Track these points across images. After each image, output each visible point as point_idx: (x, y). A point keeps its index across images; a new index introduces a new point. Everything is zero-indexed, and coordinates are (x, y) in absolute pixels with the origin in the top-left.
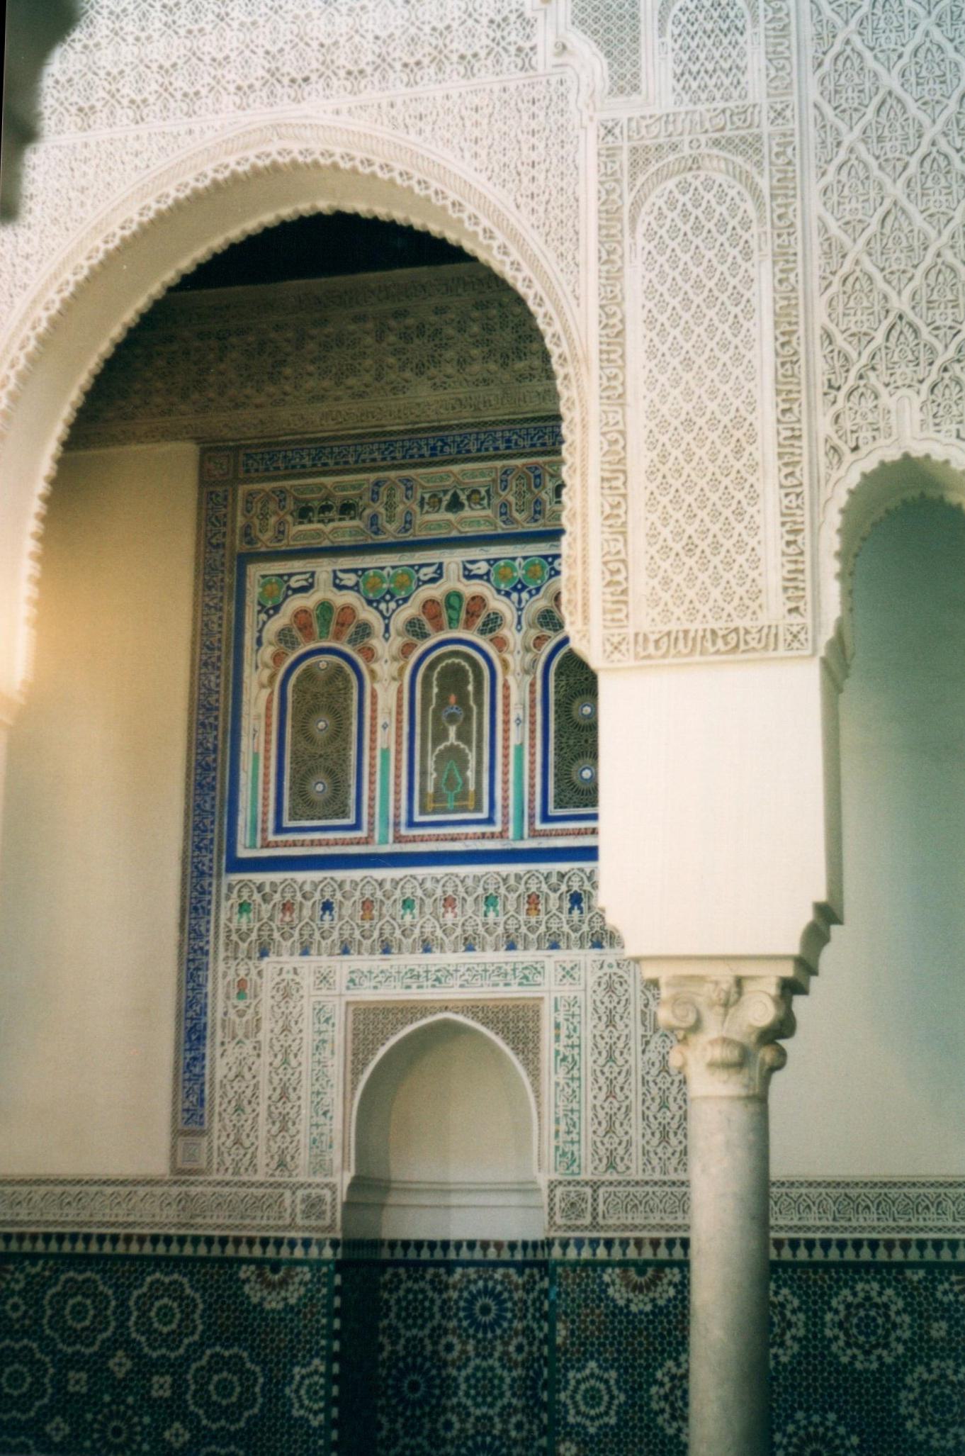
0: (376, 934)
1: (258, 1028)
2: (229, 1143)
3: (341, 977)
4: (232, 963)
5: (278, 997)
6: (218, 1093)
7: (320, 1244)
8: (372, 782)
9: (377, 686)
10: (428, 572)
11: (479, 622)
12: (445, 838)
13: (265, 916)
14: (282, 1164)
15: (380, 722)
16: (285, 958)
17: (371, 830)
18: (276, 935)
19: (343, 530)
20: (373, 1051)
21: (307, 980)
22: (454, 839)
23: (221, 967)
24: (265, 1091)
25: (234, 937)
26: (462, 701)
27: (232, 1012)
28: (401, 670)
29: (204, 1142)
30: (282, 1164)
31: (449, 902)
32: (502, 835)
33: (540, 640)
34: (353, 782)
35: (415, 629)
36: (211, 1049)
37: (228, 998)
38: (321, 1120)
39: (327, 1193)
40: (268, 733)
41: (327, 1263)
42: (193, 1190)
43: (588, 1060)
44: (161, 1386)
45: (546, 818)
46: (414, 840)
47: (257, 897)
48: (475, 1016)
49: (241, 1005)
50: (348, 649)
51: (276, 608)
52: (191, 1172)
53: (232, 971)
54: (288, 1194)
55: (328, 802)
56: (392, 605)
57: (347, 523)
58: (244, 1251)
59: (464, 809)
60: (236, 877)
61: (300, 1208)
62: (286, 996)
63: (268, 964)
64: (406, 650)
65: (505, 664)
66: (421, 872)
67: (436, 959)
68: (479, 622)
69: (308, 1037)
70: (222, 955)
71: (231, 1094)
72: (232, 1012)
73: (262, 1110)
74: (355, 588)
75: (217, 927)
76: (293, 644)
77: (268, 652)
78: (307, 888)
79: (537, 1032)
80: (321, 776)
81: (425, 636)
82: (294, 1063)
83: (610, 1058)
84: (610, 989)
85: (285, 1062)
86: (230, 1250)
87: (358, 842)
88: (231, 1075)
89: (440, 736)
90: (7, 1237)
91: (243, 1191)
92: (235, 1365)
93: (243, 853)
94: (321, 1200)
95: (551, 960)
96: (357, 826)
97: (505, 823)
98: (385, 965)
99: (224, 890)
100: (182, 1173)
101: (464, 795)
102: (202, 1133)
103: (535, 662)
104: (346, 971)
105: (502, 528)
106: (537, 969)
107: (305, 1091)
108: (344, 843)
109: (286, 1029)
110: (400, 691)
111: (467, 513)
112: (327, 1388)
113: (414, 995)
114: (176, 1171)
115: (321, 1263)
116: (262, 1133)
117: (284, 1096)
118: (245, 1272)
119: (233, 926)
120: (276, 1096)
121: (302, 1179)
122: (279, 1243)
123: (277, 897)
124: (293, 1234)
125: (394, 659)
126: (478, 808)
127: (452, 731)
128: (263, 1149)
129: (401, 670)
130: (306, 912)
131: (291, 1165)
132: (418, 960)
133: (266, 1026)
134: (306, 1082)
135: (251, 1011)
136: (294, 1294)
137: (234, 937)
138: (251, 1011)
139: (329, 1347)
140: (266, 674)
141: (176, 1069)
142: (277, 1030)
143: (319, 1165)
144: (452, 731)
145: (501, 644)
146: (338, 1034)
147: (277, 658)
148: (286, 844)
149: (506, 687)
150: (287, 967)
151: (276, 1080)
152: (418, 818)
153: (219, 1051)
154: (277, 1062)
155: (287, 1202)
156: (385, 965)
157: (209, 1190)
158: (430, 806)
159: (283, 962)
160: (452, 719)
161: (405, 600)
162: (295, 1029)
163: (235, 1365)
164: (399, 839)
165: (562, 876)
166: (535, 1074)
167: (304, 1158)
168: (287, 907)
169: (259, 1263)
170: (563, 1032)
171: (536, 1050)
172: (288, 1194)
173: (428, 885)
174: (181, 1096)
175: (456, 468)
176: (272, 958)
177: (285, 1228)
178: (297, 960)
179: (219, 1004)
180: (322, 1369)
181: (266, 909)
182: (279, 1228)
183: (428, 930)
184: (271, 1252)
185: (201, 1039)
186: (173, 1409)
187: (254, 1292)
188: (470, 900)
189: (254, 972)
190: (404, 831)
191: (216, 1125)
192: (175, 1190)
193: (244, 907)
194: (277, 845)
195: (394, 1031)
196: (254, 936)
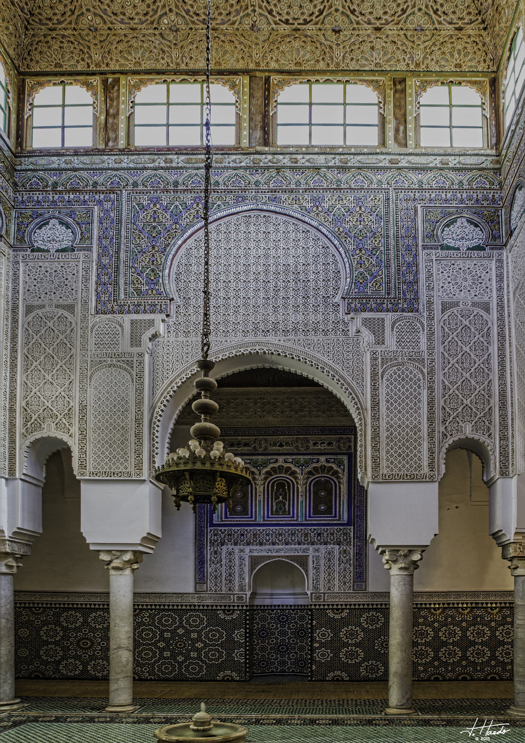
9: (257, 487)
11: (289, 472)
15: (258, 494)
21: (237, 551)
23: (209, 548)
24: (224, 574)
26: (284, 490)
29: (205, 585)
31: (280, 535)
33: (308, 478)
34: (250, 508)
35: (268, 473)
43: (322, 568)
45: (310, 517)
48: (288, 559)
55: (241, 512)
60: (212, 528)
62: (230, 554)
63: (224, 548)
65: (297, 483)
67: (276, 547)
68: (289, 472)
69: (237, 563)
70: (209, 545)
79: (307, 562)
80: (239, 506)
81: (272, 475)
83: (329, 568)
84: (329, 553)
86: (214, 608)
93: (214, 522)
95: (311, 548)
99: (209, 531)
103: (306, 483)
106: (308, 549)
107: (237, 575)
113: (270, 554)
126: (289, 514)
127: (281, 497)
129: (264, 483)
132: (271, 547)
144: (281, 497)
145: (296, 478)
149: (298, 488)
160: (281, 494)
165: (315, 529)
166: (307, 571)
170: (315, 562)
171: (307, 566)
178: (233, 546)
181: (223, 535)
185: (203, 563)
189: (219, 549)
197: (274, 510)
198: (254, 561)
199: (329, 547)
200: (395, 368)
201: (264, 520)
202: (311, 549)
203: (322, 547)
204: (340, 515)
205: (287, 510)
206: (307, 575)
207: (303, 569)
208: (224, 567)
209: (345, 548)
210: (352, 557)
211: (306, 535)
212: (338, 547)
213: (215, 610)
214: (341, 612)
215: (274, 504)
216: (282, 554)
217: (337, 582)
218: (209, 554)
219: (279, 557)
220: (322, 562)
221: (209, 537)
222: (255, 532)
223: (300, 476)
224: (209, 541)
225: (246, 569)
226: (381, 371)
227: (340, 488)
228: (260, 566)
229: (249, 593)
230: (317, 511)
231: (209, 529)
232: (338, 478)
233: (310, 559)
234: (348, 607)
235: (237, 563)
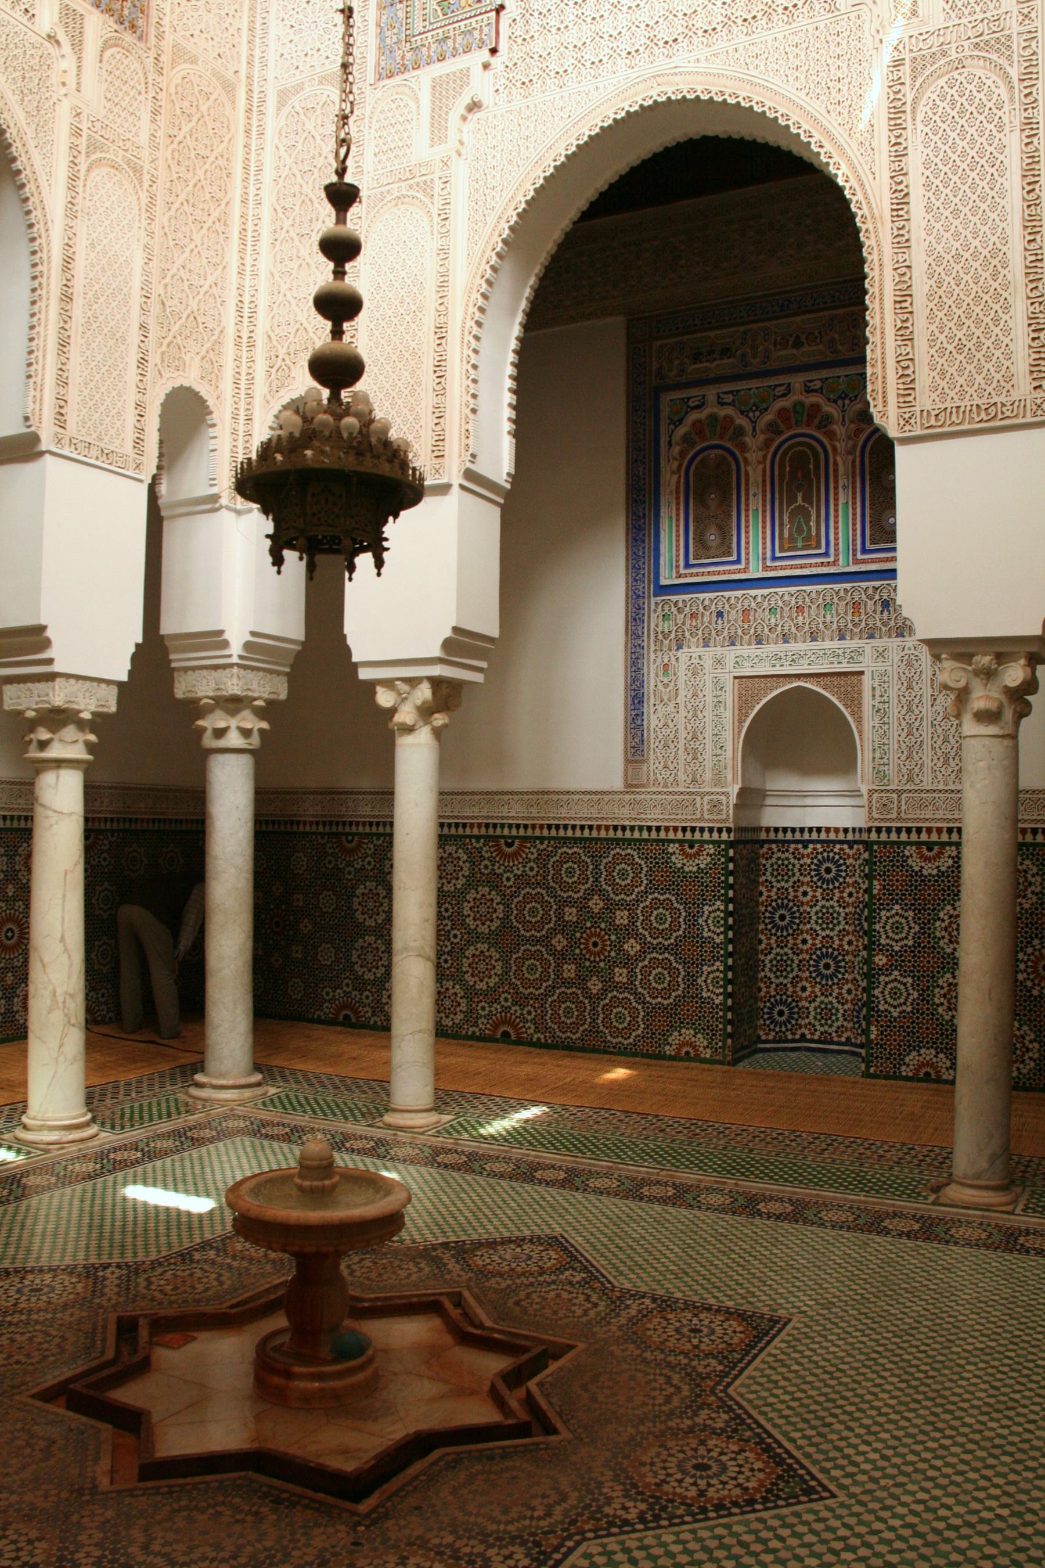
0: (752, 631)
1: (677, 695)
2: (660, 767)
4: (659, 654)
6: (652, 736)
9: (749, 469)
10: (780, 390)
11: (816, 421)
12: (796, 567)
13: (680, 622)
16: (693, 649)
17: (747, 563)
18: (687, 634)
21: (708, 663)
23: (652, 656)
24: (682, 734)
25: (660, 637)
28: (765, 457)
29: (645, 767)
31: (800, 609)
32: (835, 563)
33: (858, 432)
34: (735, 533)
35: (773, 429)
36: (648, 709)
44: (622, 918)
45: (864, 551)
46: (775, 569)
47: (674, 609)
49: (666, 681)
50: (728, 445)
51: (681, 421)
52: (636, 786)
53: (659, 660)
56: (757, 413)
57: (726, 361)
58: (671, 835)
61: (706, 807)
62: (695, 674)
64: (767, 444)
65: (834, 449)
68: (816, 421)
69: (709, 699)
70: (652, 648)
71: (660, 736)
73: (681, 746)
74: (732, 404)
77: (676, 450)
78: (707, 603)
79: (860, 693)
82: (700, 716)
83: (910, 710)
84: (909, 664)
85: (695, 715)
86: (663, 835)
87: (739, 571)
88: (661, 725)
89: (792, 499)
92: (667, 905)
93: (663, 582)
94: (720, 802)
95: (868, 647)
96: (738, 561)
97: (837, 555)
99: (653, 607)
100: (632, 785)
101: (808, 538)
102: (642, 762)
103: (854, 447)
104: (733, 656)
106: (859, 652)
107: (708, 733)
108: (730, 572)
109: (695, 695)
110: (764, 471)
111: (806, 348)
112: (725, 919)
114: (628, 785)
116: (682, 762)
117: (695, 738)
118: (672, 848)
119: (659, 630)
120: (689, 737)
121: (707, 789)
122: (693, 829)
123: (687, 609)
124: (702, 825)
125: (760, 449)
126: (818, 547)
127: (800, 498)
128: (682, 770)
129: (765, 457)
130: (706, 619)
131: (700, 781)
132: (781, 648)
133: (682, 693)
135: (672, 684)
136: (704, 861)
137: (660, 637)
138: (672, 684)
139: (726, 894)
140: (676, 463)
142: (689, 696)
145: (831, 435)
146: (729, 697)
147: (682, 454)
148: (692, 575)
149: (835, 464)
151: (689, 727)
154: (690, 716)
155: (698, 805)
158: (786, 546)
159: (692, 651)
161: (766, 409)
162: (701, 695)
163: (667, 905)
164: (766, 568)
165: (875, 589)
166: (859, 721)
168: (694, 616)
169: (681, 842)
170: (878, 693)
171: (860, 705)
172: (698, 799)
174: (630, 738)
175: (798, 319)
176: (685, 649)
179: (652, 680)
180: (722, 908)
182: (693, 820)
183: (786, 628)
184: (688, 835)
185: (641, 702)
186: (629, 931)
187: (677, 860)
188: (814, 607)
189: (673, 659)
190: (769, 563)
191: (652, 756)
192: (627, 797)
194: (686, 575)
195: (766, 695)
196: (673, 636)
197: (786, 535)
201: (766, 568)
202: (868, 649)
205: (814, 533)
208: (683, 713)
211: (856, 606)
213: (663, 841)
214: (939, 855)
215: (786, 518)
218: (652, 675)
219: (798, 676)
220: (893, 693)
222: (746, 603)
223: (839, 430)
225: (728, 716)
228: (758, 708)
231: (653, 600)
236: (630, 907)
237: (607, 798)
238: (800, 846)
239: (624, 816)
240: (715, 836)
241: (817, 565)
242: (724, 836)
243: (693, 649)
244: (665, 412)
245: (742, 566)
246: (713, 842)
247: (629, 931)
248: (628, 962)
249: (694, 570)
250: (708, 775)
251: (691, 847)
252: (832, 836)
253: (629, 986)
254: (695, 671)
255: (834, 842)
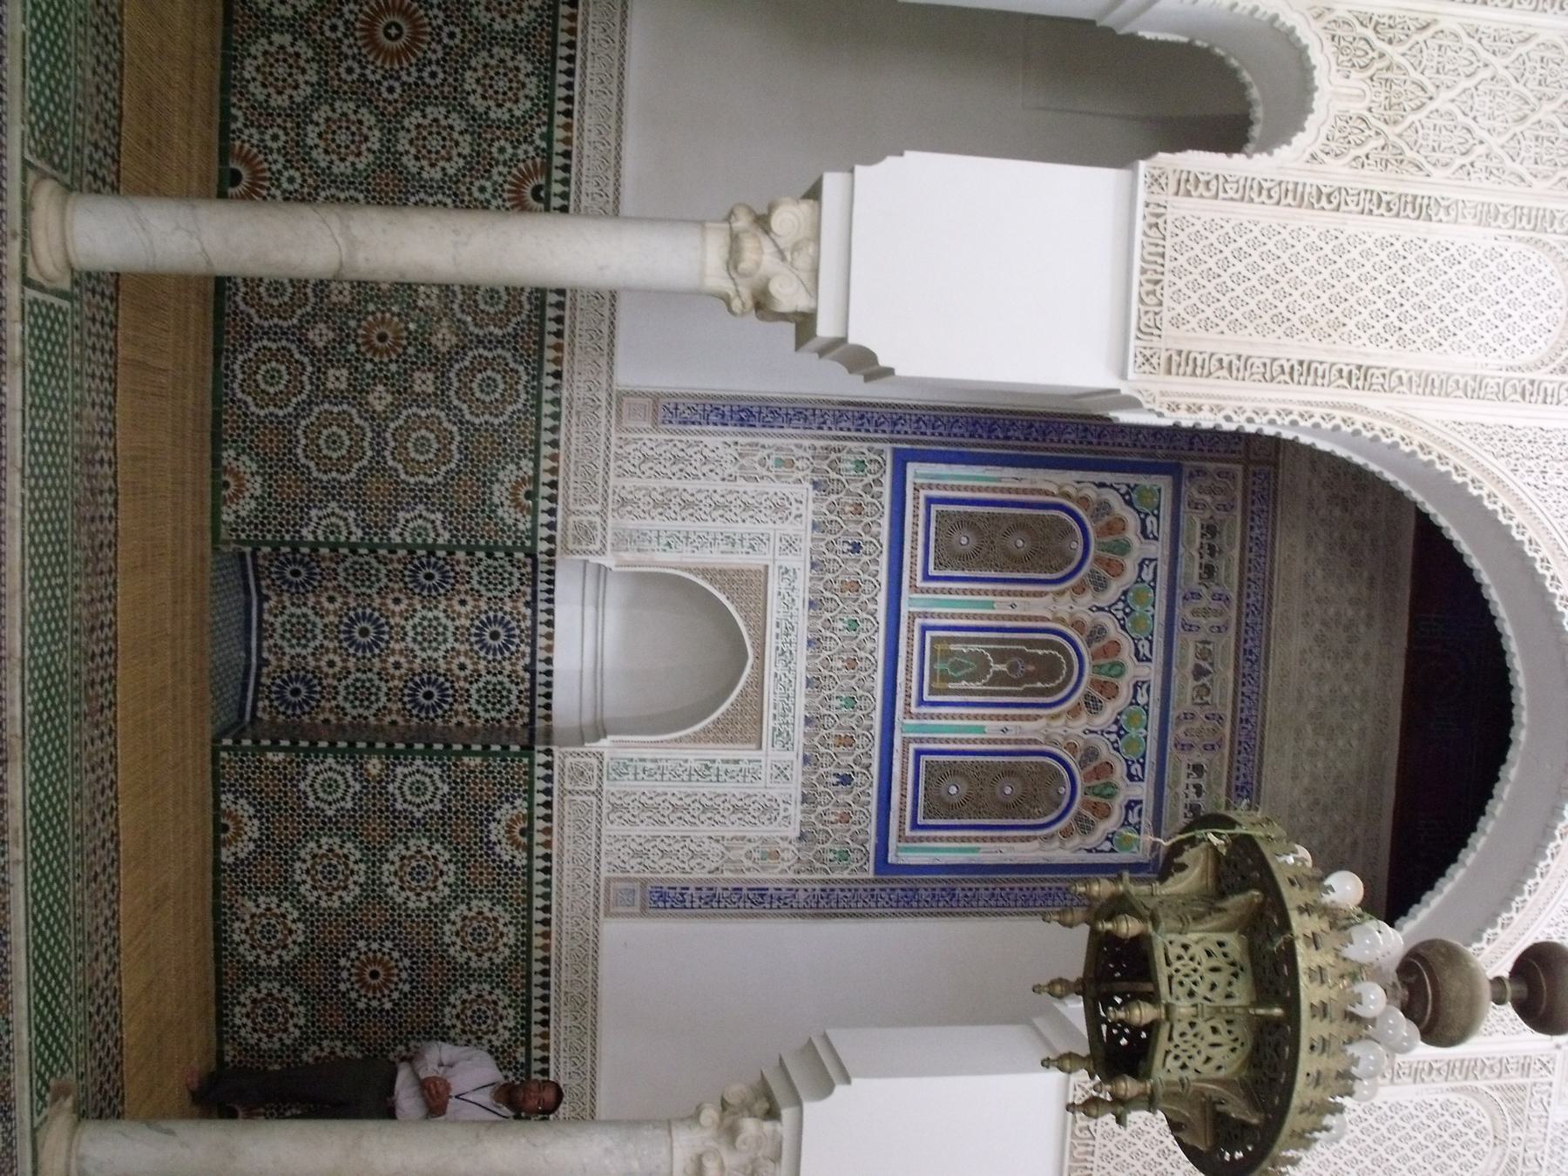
0: (828, 594)
2: (646, 450)
3: (791, 561)
4: (809, 454)
5: (776, 499)
6: (691, 438)
7: (554, 388)
8: (964, 592)
9: (1048, 599)
10: (1145, 650)
11: (1096, 694)
12: (909, 660)
13: (851, 487)
14: (624, 502)
15: (1017, 600)
16: (811, 506)
18: (833, 497)
19: (1190, 569)
20: (722, 589)
21: (789, 528)
22: (908, 669)
23: (806, 443)
24: (692, 486)
25: (833, 456)
26: (1029, 677)
27: (763, 453)
28: (1062, 621)
29: (647, 425)
30: (624, 502)
31: (852, 664)
32: (908, 713)
34: (966, 574)
35: (1097, 633)
37: (779, 449)
38: (663, 541)
39: (597, 546)
40: (1017, 491)
41: (534, 544)
42: (602, 413)
43: (706, 788)
45: (918, 753)
46: (910, 630)
47: (871, 477)
49: (770, 463)
50: (1086, 569)
52: (619, 411)
53: (800, 453)
54: (597, 508)
56: (1120, 615)
57: (1197, 571)
58: (546, 464)
59: (933, 678)
60: (888, 457)
62: (777, 508)
63: (806, 491)
64: (1078, 625)
65: (1055, 717)
66: (881, 637)
67: (802, 653)
68: (1096, 694)
69: (740, 528)
70: (819, 443)
71: (690, 451)
72: (763, 453)
73: (675, 483)
74: (1140, 580)
75: (844, 438)
76: (1095, 517)
81: (1089, 643)
82: (715, 514)
84: (765, 809)
85: (717, 506)
86: (546, 450)
88: (706, 452)
89: (1000, 656)
90: (573, 2)
91: (600, 463)
94: (592, 540)
95: (793, 757)
96: (927, 577)
97: (918, 716)
98: (799, 603)
99: (877, 446)
100: (619, 399)
101: (946, 678)
102: (655, 424)
104: (796, 565)
105: (1173, 714)
107: (690, 525)
108: (913, 564)
109: (747, 506)
110: (1044, 619)
111: (1191, 683)
112: (424, 545)
114: (621, 396)
115: (533, 536)
116: (653, 483)
117: (686, 505)
119: (843, 455)
120: (686, 496)
121: (610, 521)
122: (552, 499)
123: (868, 498)
124: (560, 513)
125: (1071, 615)
126: (933, 692)
127: (1003, 667)
129: (1062, 621)
130: (852, 528)
131: (623, 511)
132: (802, 634)
133: (751, 487)
134: (698, 526)
135: (765, 473)
136: (507, 514)
138: (765, 473)
140: (1072, 491)
141: (714, 397)
142: (745, 498)
143: (625, 540)
144: (1003, 667)
145: (1074, 713)
146: (738, 559)
148: (916, 507)
149: (1037, 718)
150: (803, 510)
151: (701, 496)
152: (928, 634)
153: (729, 439)
154: (716, 497)
155: (589, 507)
156: (799, 603)
157: (603, 430)
158: (939, 647)
160: (1013, 668)
161: (1123, 627)
162: (745, 515)
164: (912, 616)
165: (868, 767)
166: (695, 739)
167: (630, 523)
168: (858, 509)
169: (535, 479)
170: (731, 767)
171: (716, 740)
172: (597, 508)
173: (869, 645)
174: (691, 402)
175: (1230, 674)
176: (812, 494)
177: (566, 505)
178: (809, 517)
179: (772, 441)
180: (440, 541)
181: (857, 487)
182: (566, 498)
183: (828, 644)
184: (545, 491)
185: (742, 422)
186: (402, 391)
187: (508, 474)
188: (853, 683)
189: (800, 475)
190: (918, 621)
191: (662, 437)
192: (603, 396)
193: (860, 466)
194: (916, 498)
195: (739, 609)
196: (833, 475)
197: (953, 647)
198: (750, 585)
199: (796, 811)
200: (1487, 1122)
201: (912, 616)
203: (795, 789)
204: (921, 839)
205: (951, 686)
206: (680, 740)
207: (706, 731)
209: (785, 855)
210: (749, 875)
211: (848, 742)
212: (793, 832)
213: (537, 451)
215: (974, 647)
216: (771, 667)
217: (646, 830)
219: (760, 657)
220: (729, 787)
221: (849, 444)
223: (1078, 726)
224: (834, 444)
225: (713, 557)
226: (1481, 1084)
227: (1028, 839)
228: (722, 598)
229: (608, 561)
230: (939, 774)
232: (1067, 833)
233: (745, 753)
234: (539, 864)
235: (740, 528)
236: (440, 396)
237: (603, 361)
238: (529, 598)
239: (576, 388)
240: (543, 532)
241: (908, 688)
242: (543, 546)
243: (811, 506)
244: (1144, 481)
245: (920, 583)
246: (534, 529)
247: (402, 391)
248: (357, 392)
249: (922, 512)
250: (630, 523)
251: (528, 495)
252: (542, 642)
253: (322, 393)
254: (780, 508)
255: (533, 645)
